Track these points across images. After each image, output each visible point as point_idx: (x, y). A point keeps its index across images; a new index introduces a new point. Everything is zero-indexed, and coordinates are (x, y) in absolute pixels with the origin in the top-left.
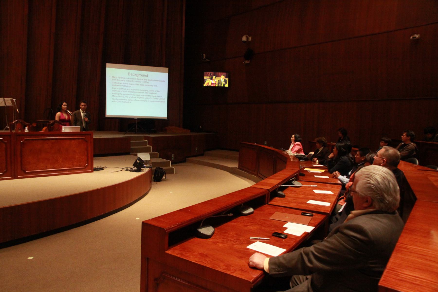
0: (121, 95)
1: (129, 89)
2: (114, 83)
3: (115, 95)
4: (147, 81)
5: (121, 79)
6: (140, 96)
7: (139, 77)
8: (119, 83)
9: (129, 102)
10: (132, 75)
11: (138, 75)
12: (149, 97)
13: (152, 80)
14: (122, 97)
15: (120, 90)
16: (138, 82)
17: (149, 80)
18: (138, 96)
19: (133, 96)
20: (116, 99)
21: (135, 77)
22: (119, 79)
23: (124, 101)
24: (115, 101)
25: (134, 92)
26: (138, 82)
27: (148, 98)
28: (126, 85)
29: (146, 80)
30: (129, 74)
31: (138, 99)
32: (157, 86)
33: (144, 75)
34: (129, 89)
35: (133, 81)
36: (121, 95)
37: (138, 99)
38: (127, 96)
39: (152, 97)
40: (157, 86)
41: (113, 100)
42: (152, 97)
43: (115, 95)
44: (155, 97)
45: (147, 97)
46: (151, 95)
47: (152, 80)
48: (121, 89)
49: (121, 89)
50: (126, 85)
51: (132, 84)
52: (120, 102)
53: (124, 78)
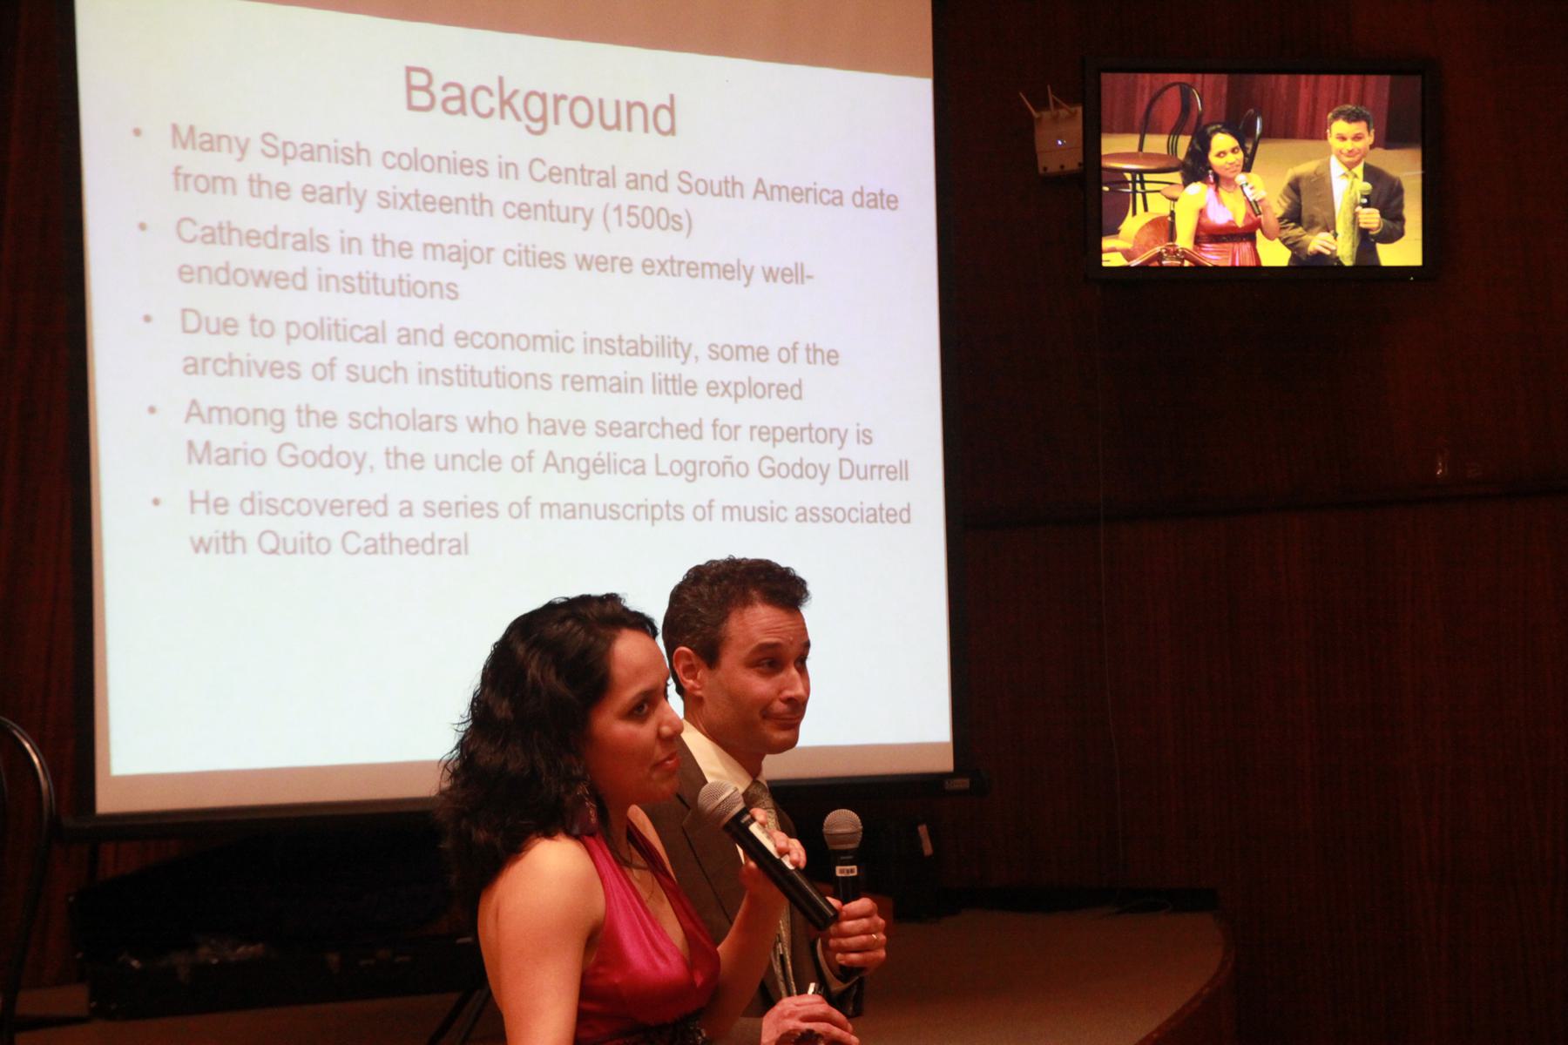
0: (314, 438)
1: (435, 337)
2: (216, 234)
3: (224, 435)
4: (674, 201)
5: (300, 173)
6: (589, 446)
7: (566, 144)
8: (276, 238)
9: (432, 545)
10: (461, 101)
11: (542, 111)
12: (710, 449)
13: (729, 187)
14: (330, 458)
15: (308, 352)
16: (549, 211)
17: (691, 185)
18: (566, 445)
19: (493, 442)
20: (255, 504)
21: (501, 138)
22: (274, 171)
23: (372, 527)
24: (230, 542)
25: (500, 379)
26: (549, 211)
27: (691, 470)
28: (390, 267)
29: (659, 182)
30: (419, 87)
31: (566, 488)
32: (795, 274)
33: (623, 116)
34: (435, 337)
35: (479, 204)
36: (314, 438)
37: (566, 488)
38: (410, 441)
39: (747, 450)
40: (795, 274)
41: (208, 524)
42: (747, 450)
43: (224, 435)
44: (787, 452)
45: (687, 450)
46: (727, 411)
47: (729, 187)
48: (325, 330)
49: (325, 330)
50: (390, 267)
51: (461, 255)
52: (310, 544)
53: (354, 155)
